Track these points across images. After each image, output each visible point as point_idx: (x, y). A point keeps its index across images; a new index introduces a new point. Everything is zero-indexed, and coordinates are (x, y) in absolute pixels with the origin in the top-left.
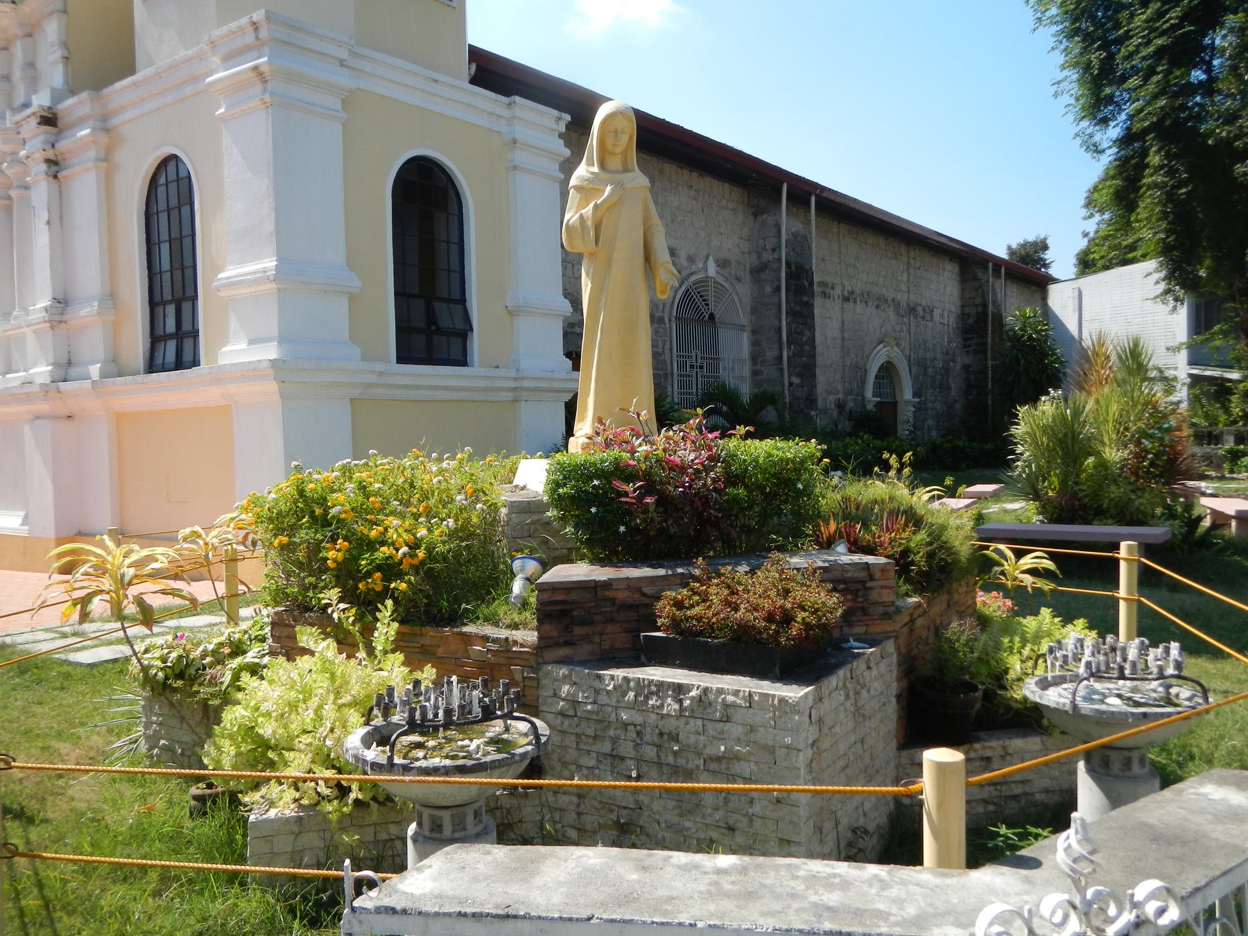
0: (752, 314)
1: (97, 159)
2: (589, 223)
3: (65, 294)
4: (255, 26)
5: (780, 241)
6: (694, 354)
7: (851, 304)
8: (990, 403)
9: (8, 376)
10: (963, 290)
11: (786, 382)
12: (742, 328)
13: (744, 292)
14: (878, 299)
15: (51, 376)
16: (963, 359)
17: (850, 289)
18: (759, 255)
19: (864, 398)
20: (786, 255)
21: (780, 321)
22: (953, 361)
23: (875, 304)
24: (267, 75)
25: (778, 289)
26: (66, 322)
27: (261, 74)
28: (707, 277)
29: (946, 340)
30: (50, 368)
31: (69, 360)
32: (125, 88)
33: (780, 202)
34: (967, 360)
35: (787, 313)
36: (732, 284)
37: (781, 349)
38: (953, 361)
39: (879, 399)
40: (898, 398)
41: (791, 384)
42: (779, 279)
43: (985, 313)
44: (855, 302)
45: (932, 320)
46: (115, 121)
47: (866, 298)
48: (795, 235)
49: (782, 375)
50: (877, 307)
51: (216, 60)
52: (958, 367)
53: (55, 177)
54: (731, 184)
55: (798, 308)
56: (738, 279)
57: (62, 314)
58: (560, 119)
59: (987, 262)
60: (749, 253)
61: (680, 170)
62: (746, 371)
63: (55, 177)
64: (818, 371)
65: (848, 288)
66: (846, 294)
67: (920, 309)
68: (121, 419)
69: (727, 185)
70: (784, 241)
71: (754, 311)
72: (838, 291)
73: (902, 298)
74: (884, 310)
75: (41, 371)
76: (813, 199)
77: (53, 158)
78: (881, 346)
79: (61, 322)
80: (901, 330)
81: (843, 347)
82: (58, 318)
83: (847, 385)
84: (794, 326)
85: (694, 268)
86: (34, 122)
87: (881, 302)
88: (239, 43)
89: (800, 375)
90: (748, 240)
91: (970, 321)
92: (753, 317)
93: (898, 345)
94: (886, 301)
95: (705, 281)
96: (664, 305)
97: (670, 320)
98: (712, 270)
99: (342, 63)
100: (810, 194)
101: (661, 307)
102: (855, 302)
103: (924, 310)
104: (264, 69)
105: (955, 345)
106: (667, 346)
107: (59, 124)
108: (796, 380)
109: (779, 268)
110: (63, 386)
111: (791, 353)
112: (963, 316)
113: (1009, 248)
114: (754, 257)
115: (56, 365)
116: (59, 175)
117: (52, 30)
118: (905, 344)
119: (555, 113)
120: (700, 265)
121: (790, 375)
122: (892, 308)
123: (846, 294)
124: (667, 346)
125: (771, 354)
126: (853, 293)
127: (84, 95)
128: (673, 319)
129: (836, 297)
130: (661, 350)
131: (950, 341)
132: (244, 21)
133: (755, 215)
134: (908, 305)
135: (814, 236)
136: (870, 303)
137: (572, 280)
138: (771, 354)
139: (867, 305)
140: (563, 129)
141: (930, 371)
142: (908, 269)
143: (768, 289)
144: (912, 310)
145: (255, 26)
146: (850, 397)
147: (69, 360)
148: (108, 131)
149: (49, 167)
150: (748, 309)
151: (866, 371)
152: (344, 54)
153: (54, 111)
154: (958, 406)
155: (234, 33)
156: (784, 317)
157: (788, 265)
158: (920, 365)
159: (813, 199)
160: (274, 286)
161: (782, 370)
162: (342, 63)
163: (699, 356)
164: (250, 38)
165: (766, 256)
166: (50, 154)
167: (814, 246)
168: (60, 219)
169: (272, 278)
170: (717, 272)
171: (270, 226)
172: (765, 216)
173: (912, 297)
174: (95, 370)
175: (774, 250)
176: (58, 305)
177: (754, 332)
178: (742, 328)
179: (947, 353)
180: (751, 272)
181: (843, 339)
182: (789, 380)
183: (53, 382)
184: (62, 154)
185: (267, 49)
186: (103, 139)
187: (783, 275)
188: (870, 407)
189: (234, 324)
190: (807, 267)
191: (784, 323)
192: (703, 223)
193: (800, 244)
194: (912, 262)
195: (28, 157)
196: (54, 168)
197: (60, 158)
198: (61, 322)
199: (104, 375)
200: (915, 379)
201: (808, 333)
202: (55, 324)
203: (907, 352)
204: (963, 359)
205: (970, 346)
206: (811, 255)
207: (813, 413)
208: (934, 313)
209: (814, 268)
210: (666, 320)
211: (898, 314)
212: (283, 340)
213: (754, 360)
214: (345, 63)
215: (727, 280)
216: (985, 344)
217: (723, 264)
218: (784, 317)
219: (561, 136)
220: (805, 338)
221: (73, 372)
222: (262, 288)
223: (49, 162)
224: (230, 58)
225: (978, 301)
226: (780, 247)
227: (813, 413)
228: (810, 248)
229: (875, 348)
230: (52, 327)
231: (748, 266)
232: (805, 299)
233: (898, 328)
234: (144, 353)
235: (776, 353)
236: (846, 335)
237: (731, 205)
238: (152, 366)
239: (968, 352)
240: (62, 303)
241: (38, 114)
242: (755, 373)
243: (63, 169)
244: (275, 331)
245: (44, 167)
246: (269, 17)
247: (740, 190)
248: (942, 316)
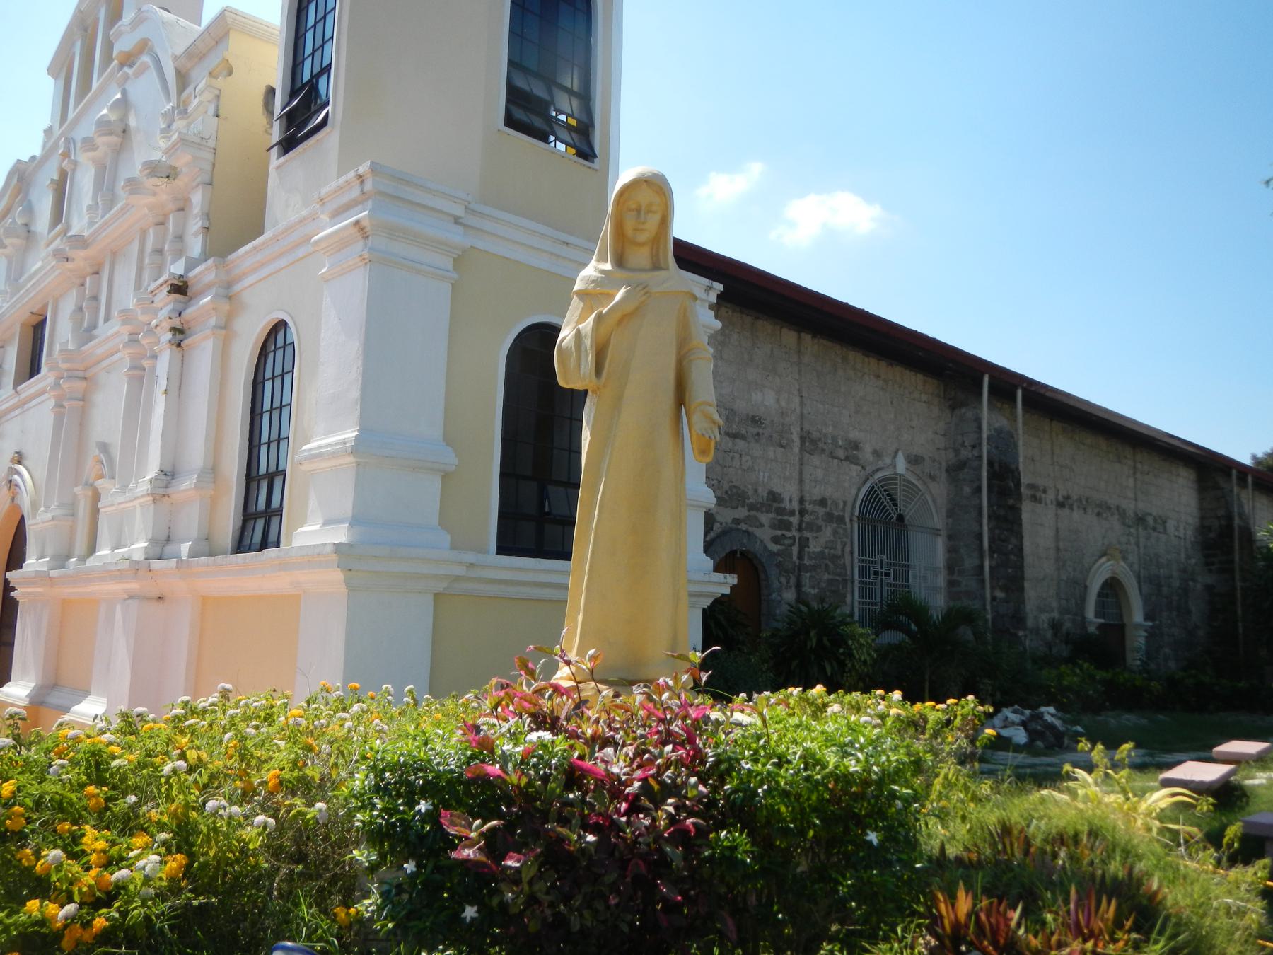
0: (948, 517)
1: (217, 327)
2: (588, 342)
3: (174, 466)
5: (980, 438)
6: (878, 559)
7: (1066, 511)
8: (1241, 630)
9: (116, 551)
10: (1201, 500)
11: (988, 596)
12: (936, 532)
13: (938, 492)
14: (1099, 506)
15: (146, 553)
16: (1204, 579)
17: (1065, 493)
18: (957, 452)
19: (1084, 618)
20: (989, 453)
21: (981, 525)
22: (1194, 580)
23: (1096, 510)
24: (368, 229)
25: (979, 489)
27: (362, 229)
28: (896, 474)
29: (1183, 556)
30: (146, 544)
31: (169, 537)
32: (247, 253)
33: (980, 394)
34: (1209, 579)
35: (989, 517)
36: (925, 483)
37: (981, 557)
38: (1194, 580)
39: (1102, 621)
40: (1126, 620)
41: (994, 599)
42: (980, 479)
43: (1230, 527)
44: (1071, 508)
45: (1165, 532)
46: (237, 288)
47: (1084, 504)
48: (999, 431)
49: (983, 588)
50: (1098, 514)
51: (324, 218)
52: (1199, 587)
53: (179, 345)
54: (924, 375)
55: (1002, 512)
56: (932, 478)
57: (167, 487)
58: (710, 288)
59: (1230, 468)
60: (946, 449)
61: (866, 359)
62: (941, 581)
63: (179, 345)
64: (1027, 585)
65: (1063, 493)
66: (1061, 499)
67: (1150, 520)
68: (207, 604)
69: (920, 376)
70: (985, 436)
71: (950, 513)
72: (1050, 496)
73: (1129, 506)
74: (1106, 519)
75: (138, 547)
76: (1019, 393)
77: (179, 326)
78: (1104, 559)
79: (164, 495)
80: (1128, 543)
81: (1057, 559)
82: (162, 491)
83: (1064, 602)
84: (997, 531)
85: (880, 464)
86: (166, 289)
87: (1103, 509)
88: (345, 199)
89: (1005, 589)
90: (944, 435)
91: (1212, 535)
92: (950, 520)
93: (1124, 559)
94: (1109, 508)
95: (893, 478)
96: (845, 503)
97: (851, 520)
98: (901, 466)
99: (457, 220)
100: (1016, 387)
101: (841, 505)
102: (1071, 508)
103: (1155, 520)
104: (366, 223)
105: (1193, 561)
106: (848, 549)
108: (1000, 594)
109: (980, 467)
110: (156, 564)
111: (994, 563)
112: (1203, 529)
113: (1254, 457)
114: (951, 455)
115: (153, 541)
116: (183, 344)
118: (1133, 558)
119: (705, 281)
120: (888, 460)
121: (992, 588)
122: (1116, 517)
123: (1061, 499)
124: (848, 549)
125: (969, 563)
126: (1068, 498)
128: (856, 519)
129: (1049, 502)
130: (839, 553)
131: (1188, 557)
132: (351, 174)
133: (953, 408)
134: (1136, 514)
135: (1020, 431)
136: (1089, 510)
137: (740, 472)
138: (969, 563)
139: (1085, 512)
140: (714, 299)
141: (1165, 590)
142: (1134, 473)
143: (967, 490)
144: (1141, 520)
146: (1067, 617)
147: (169, 537)
148: (230, 298)
149: (174, 335)
150: (944, 511)
151: (1086, 587)
152: (459, 211)
153: (185, 279)
154: (1201, 633)
155: (342, 188)
156: (985, 521)
157: (990, 463)
158: (1152, 584)
159: (1019, 393)
160: (351, 459)
161: (983, 581)
162: (457, 220)
163: (885, 561)
165: (965, 454)
166: (176, 323)
167: (1021, 443)
168: (179, 387)
169: (350, 450)
170: (907, 469)
171: (355, 393)
172: (963, 410)
173: (1141, 505)
174: (185, 548)
175: (974, 447)
176: (164, 477)
177: (950, 537)
178: (936, 532)
179: (1185, 571)
180: (947, 471)
181: (1058, 549)
182: (992, 593)
183: (146, 559)
184: (187, 322)
187: (985, 474)
188: (1092, 629)
189: (313, 503)
190: (1013, 467)
191: (985, 529)
192: (892, 416)
193: (1003, 441)
194: (1139, 466)
195: (157, 326)
196: (179, 337)
197: (186, 327)
198: (164, 495)
199: (194, 554)
200: (1146, 600)
201: (1014, 541)
202: (158, 497)
203: (1136, 567)
204: (1204, 579)
205: (1213, 564)
206: (1017, 454)
207: (1021, 633)
208: (1168, 525)
209: (1021, 468)
210: (847, 520)
211: (1124, 524)
212: (356, 521)
213: (951, 568)
214: (461, 221)
215: (919, 478)
216: (1232, 561)
217: (914, 460)
218: (985, 521)
219: (711, 307)
220: (1010, 547)
221: (169, 549)
222: (341, 461)
223: (175, 330)
224: (337, 214)
225: (1221, 512)
226: (980, 444)
227: (1021, 633)
228: (1016, 446)
229: (1097, 561)
230: (154, 501)
231: (944, 464)
232: (1011, 502)
233: (1124, 539)
234: (233, 532)
235: (977, 562)
236: (1061, 545)
237: (924, 397)
238: (241, 546)
239: (1210, 571)
240: (169, 475)
241: (169, 282)
242: (951, 584)
243: (186, 338)
244: (349, 513)
245: (169, 335)
246: (374, 169)
247: (935, 381)
248: (1177, 529)
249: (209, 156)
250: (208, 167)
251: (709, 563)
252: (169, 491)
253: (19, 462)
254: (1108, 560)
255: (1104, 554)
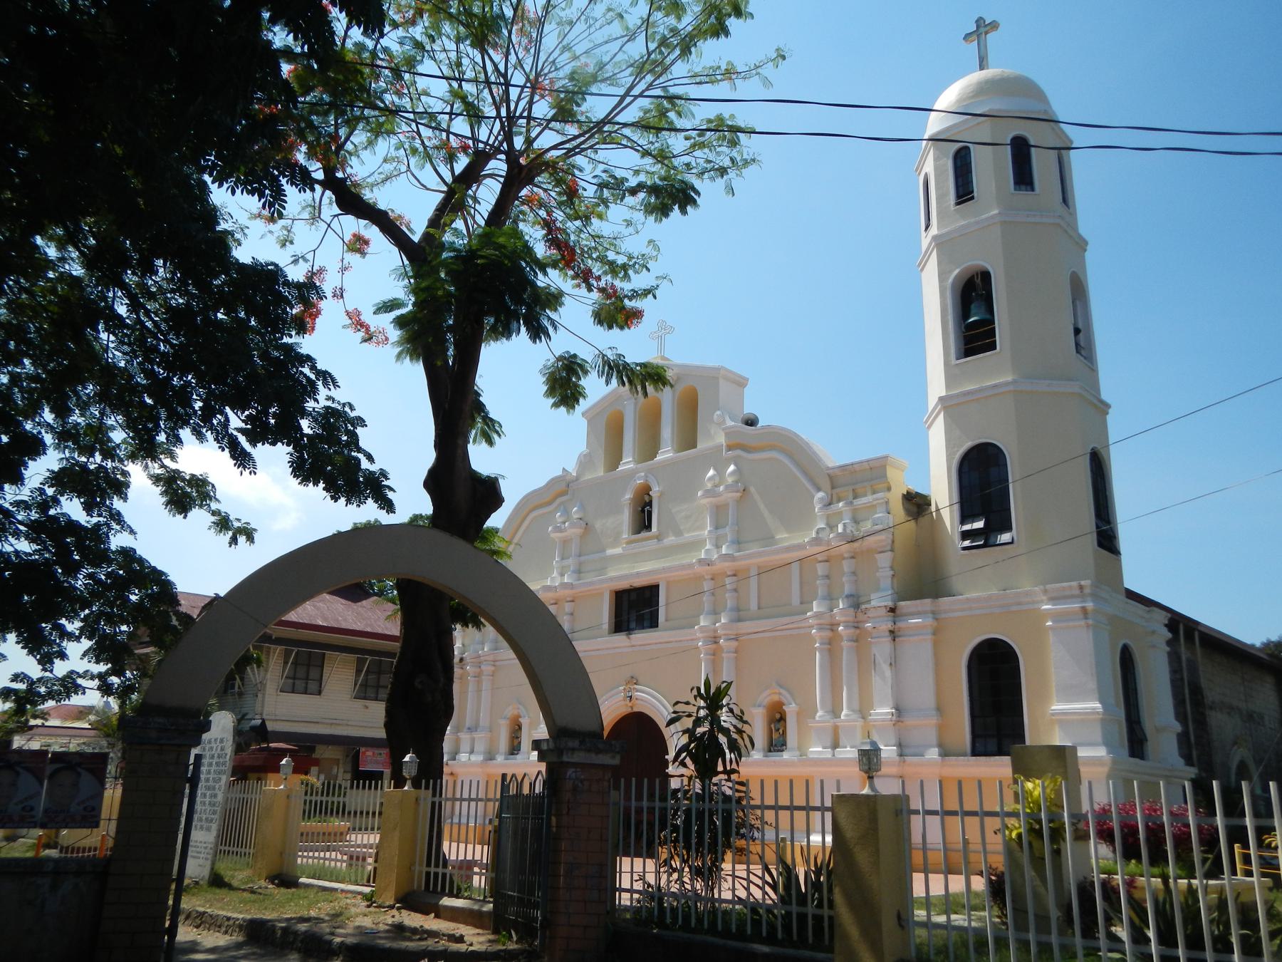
3: (897, 705)
4: (1081, 587)
26: (902, 722)
42: (1184, 695)
63: (894, 640)
67: (1255, 715)
70: (1184, 665)
86: (883, 612)
88: (1068, 593)
107: (898, 612)
117: (884, 560)
127: (928, 601)
132: (1074, 584)
140: (1167, 622)
145: (1081, 587)
148: (937, 619)
164: (1077, 592)
166: (892, 629)
171: (1092, 685)
174: (933, 754)
184: (899, 628)
185: (1089, 599)
186: (935, 624)
187: (1187, 691)
212: (1107, 743)
219: (1166, 625)
223: (892, 632)
226: (1181, 670)
240: (899, 710)
243: (900, 636)
244: (1099, 738)
245: (887, 633)
249: (891, 536)
250: (890, 542)
251: (1182, 761)
252: (901, 719)
253: (635, 684)
254: (1239, 748)
255: (1235, 743)
